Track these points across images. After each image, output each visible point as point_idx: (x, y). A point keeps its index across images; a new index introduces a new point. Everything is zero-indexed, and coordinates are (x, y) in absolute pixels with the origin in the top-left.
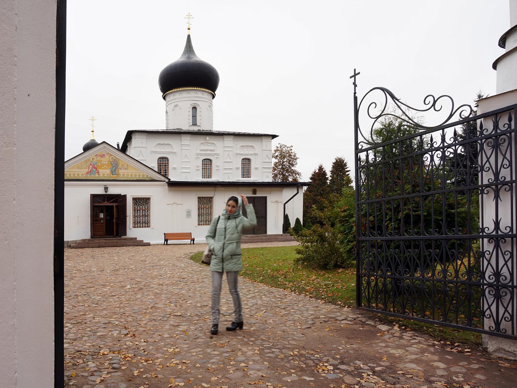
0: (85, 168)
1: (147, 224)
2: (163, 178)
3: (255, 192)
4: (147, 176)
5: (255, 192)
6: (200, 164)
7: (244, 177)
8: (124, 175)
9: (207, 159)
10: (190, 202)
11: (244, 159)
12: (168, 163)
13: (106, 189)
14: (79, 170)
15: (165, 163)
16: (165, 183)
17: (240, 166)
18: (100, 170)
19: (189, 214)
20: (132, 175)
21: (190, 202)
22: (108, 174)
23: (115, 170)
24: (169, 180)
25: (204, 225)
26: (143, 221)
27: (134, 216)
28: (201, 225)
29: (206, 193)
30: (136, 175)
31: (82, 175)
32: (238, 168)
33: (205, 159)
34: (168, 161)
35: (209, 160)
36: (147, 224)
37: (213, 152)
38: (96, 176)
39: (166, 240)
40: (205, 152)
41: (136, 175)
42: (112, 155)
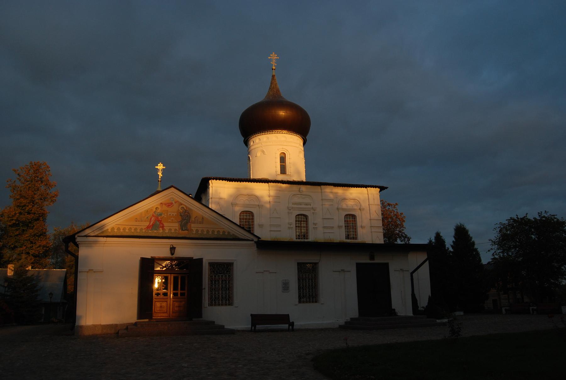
0: (145, 221)
1: (228, 300)
2: (251, 237)
3: (372, 258)
4: (229, 233)
5: (372, 258)
6: (293, 220)
7: (348, 238)
8: (197, 231)
9: (301, 215)
10: (287, 269)
11: (346, 215)
12: (253, 219)
13: (173, 249)
14: (137, 223)
15: (250, 219)
16: (253, 242)
17: (342, 223)
18: (165, 224)
19: (286, 287)
20: (208, 231)
21: (287, 269)
22: (176, 230)
23: (186, 223)
24: (259, 238)
25: (307, 302)
26: (225, 296)
27: (211, 289)
28: (304, 302)
29: (308, 258)
30: (213, 231)
31: (141, 229)
32: (340, 227)
33: (298, 215)
34: (253, 216)
35: (304, 215)
36: (228, 300)
37: (309, 206)
38: (160, 232)
39: (254, 324)
40: (299, 206)
41: (213, 231)
42: (181, 204)
